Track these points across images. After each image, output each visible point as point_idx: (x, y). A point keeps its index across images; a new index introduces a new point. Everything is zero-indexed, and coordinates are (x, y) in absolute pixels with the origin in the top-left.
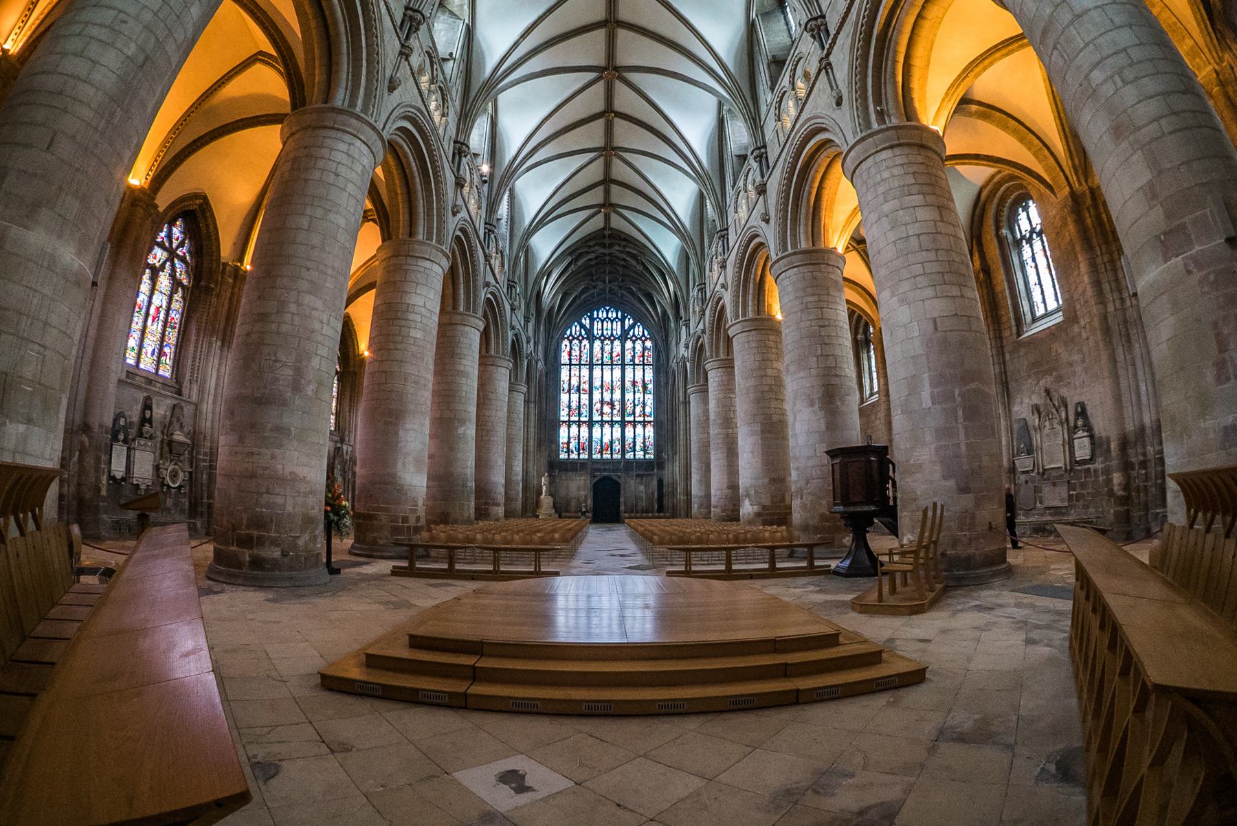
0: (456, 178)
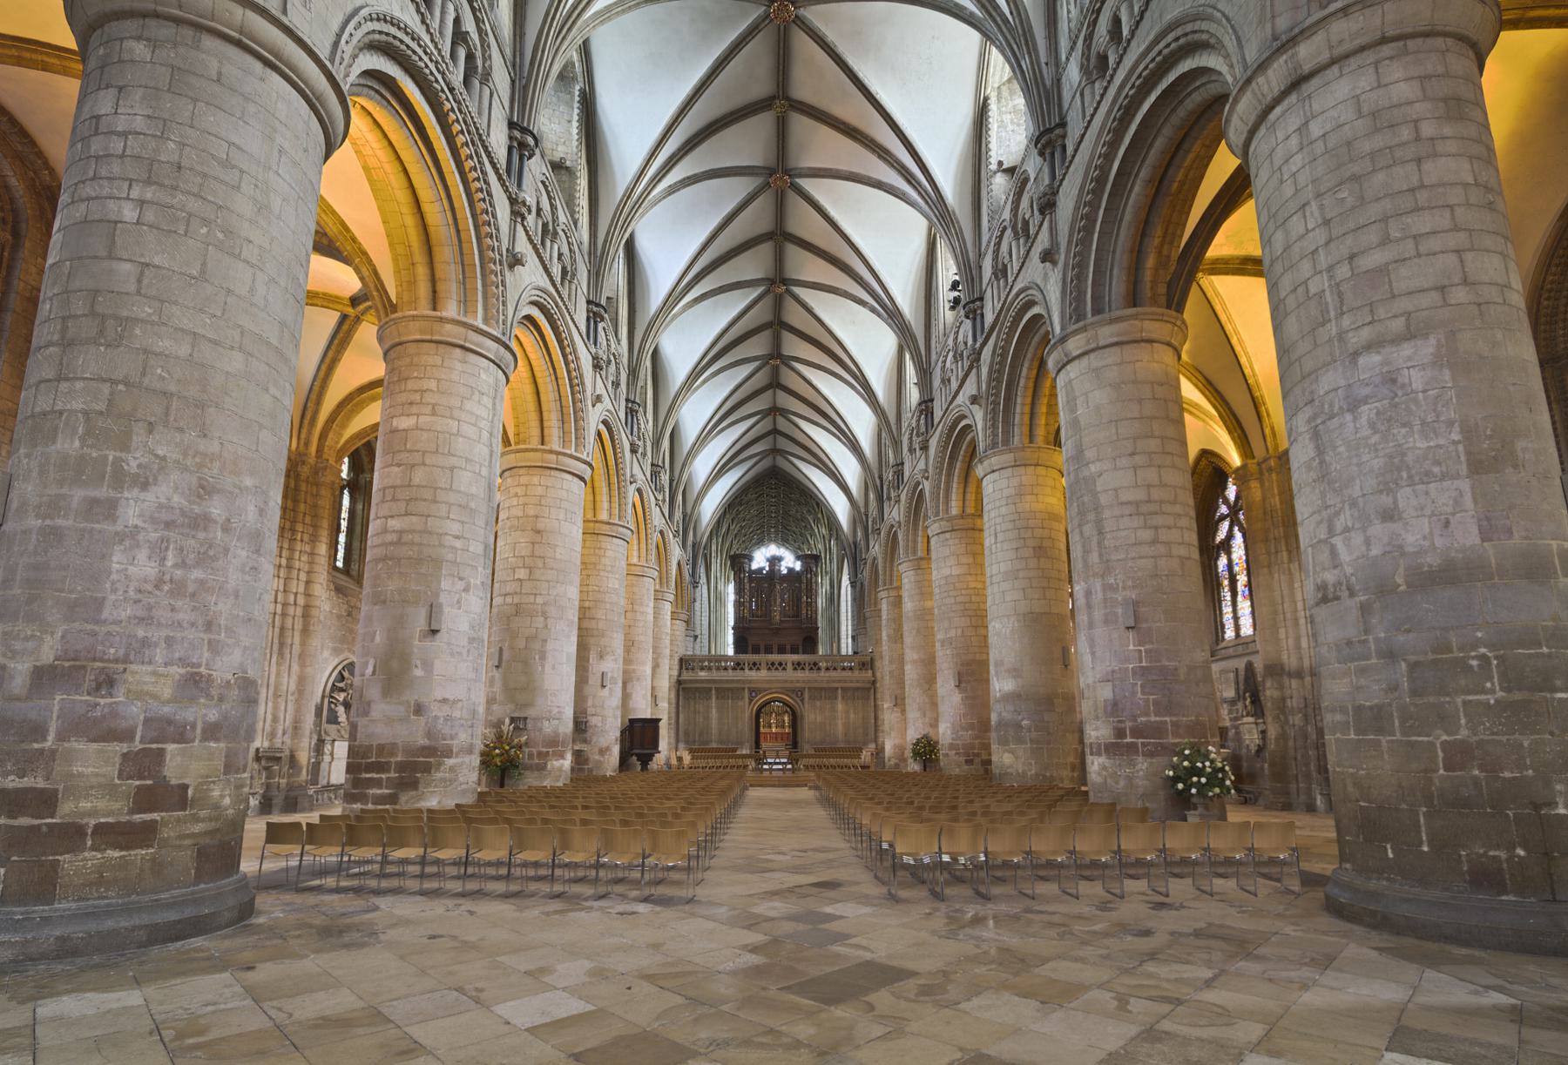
0: (594, 358)
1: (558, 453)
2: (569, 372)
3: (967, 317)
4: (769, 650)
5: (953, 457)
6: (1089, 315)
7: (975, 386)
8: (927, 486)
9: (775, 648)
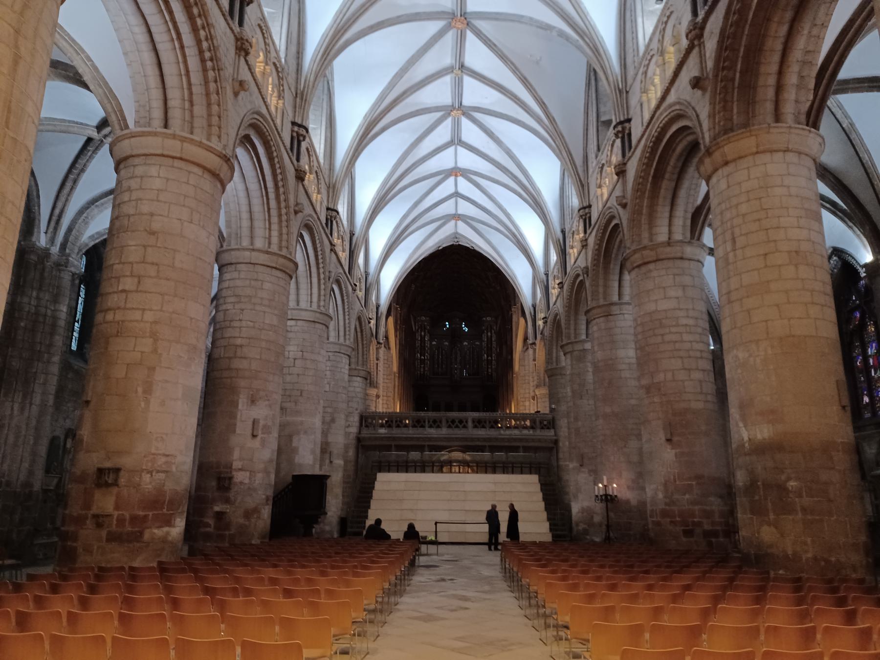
0: (237, 40)
1: (183, 140)
2: (199, 42)
4: (449, 408)
5: (658, 177)
7: (698, 67)
8: (624, 216)
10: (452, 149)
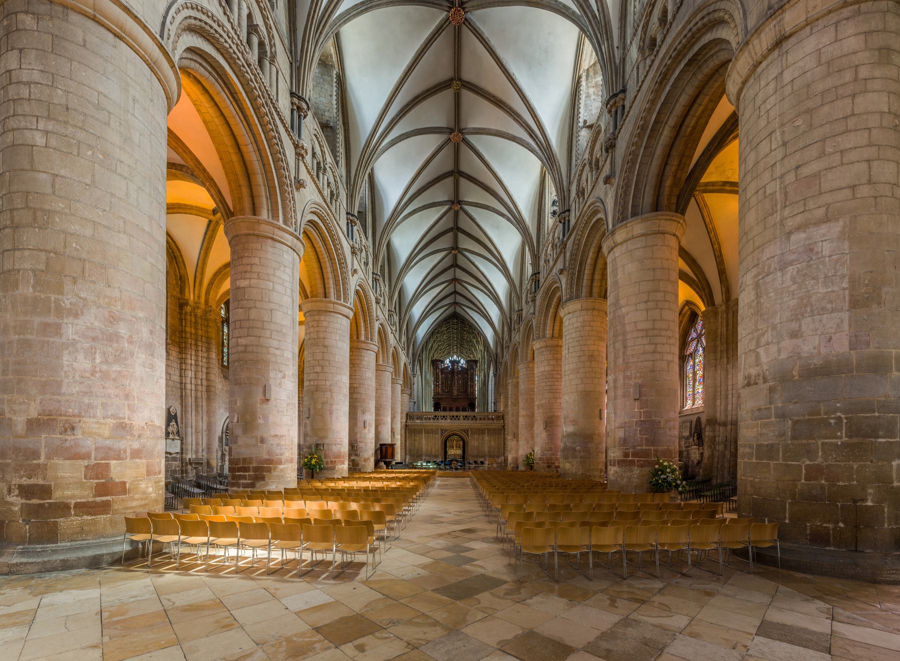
3: (560, 222)
4: (451, 410)
6: (630, 216)
9: (454, 409)
10: (452, 270)
